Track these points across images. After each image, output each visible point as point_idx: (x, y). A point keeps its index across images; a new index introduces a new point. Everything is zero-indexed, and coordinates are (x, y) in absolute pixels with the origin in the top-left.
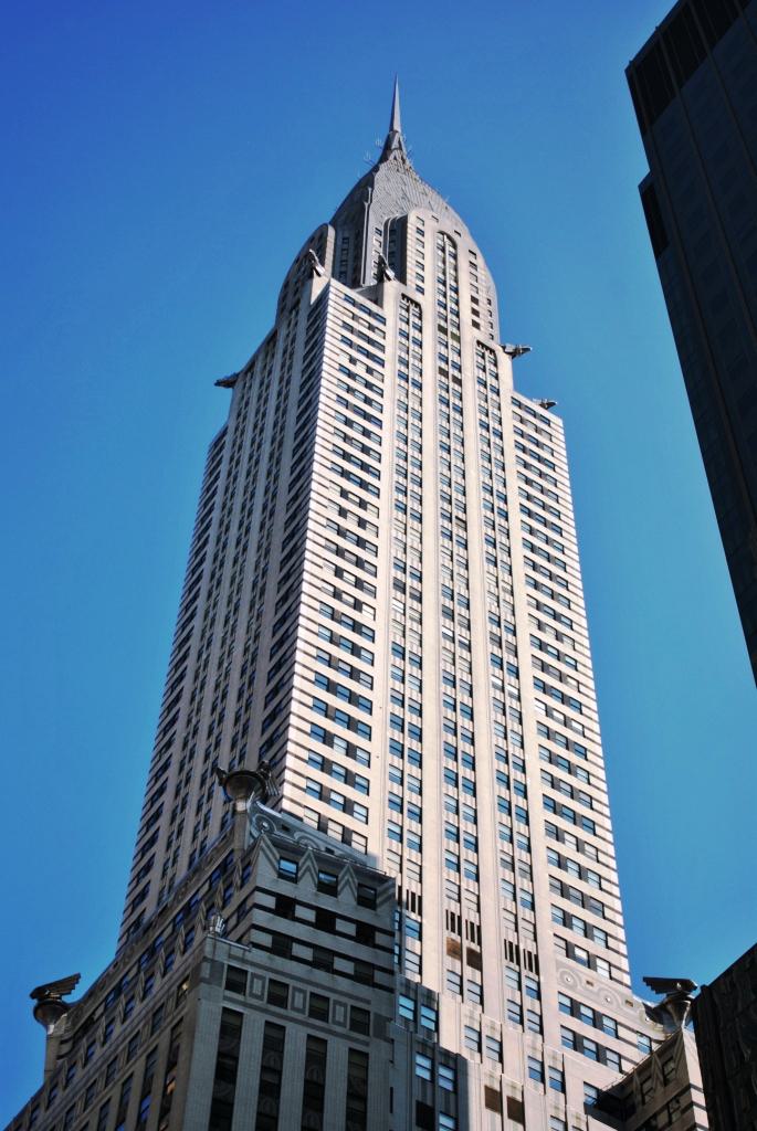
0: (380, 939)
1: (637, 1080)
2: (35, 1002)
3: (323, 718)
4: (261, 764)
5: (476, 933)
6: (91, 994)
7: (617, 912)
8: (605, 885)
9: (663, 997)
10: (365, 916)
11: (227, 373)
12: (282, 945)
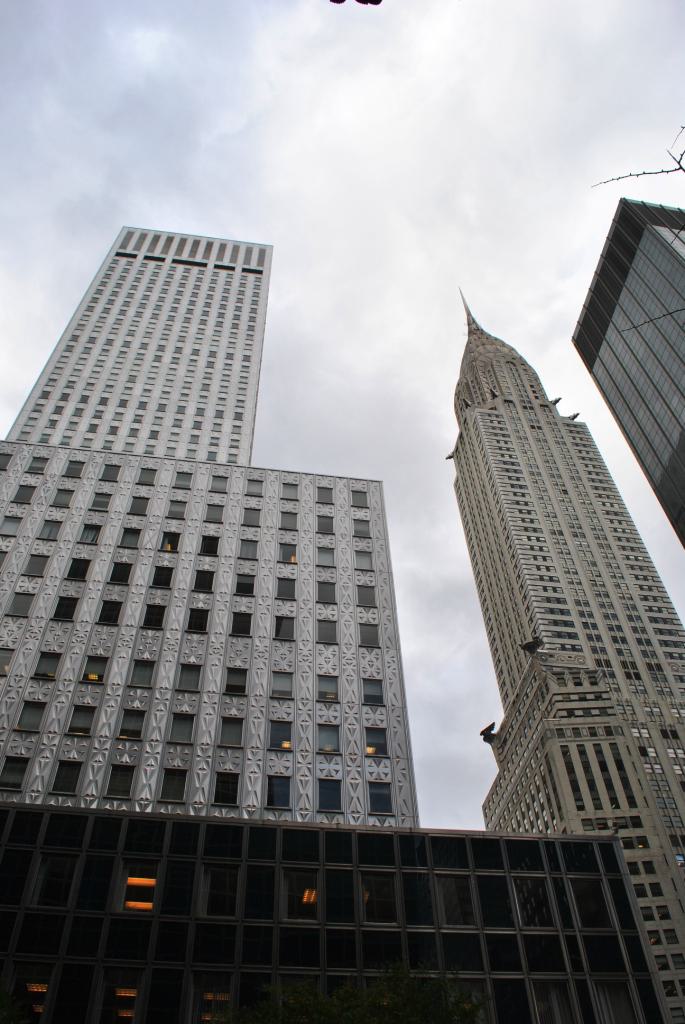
0: (604, 696)
4: (534, 638)
5: (634, 665)
6: (503, 728)
10: (595, 689)
12: (571, 713)
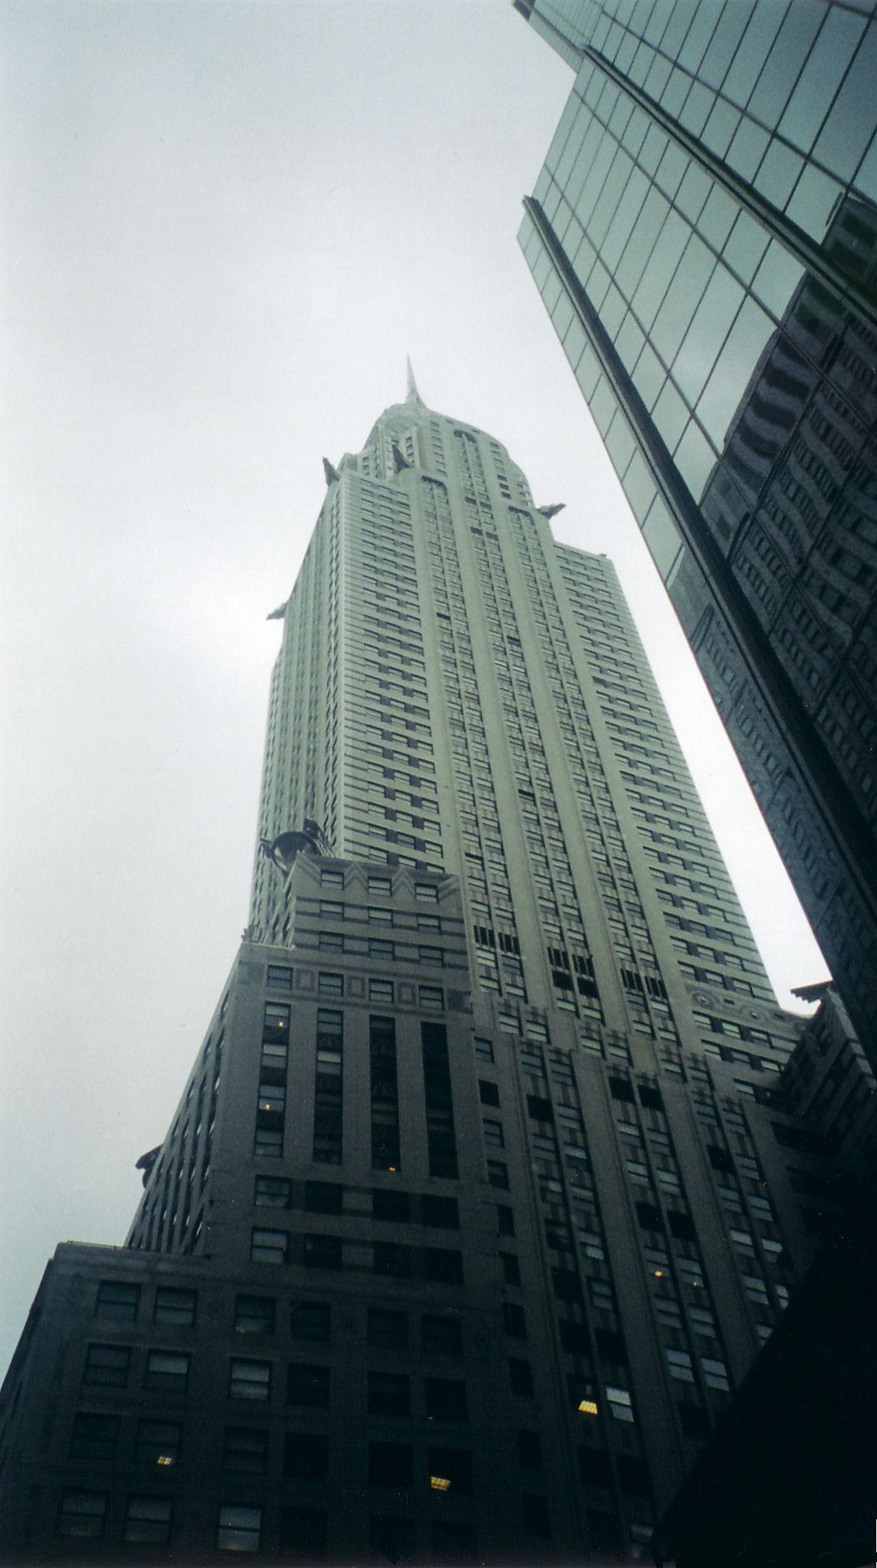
1: (795, 1066)
2: (143, 1171)
5: (586, 965)
9: (818, 1003)
11: (277, 605)
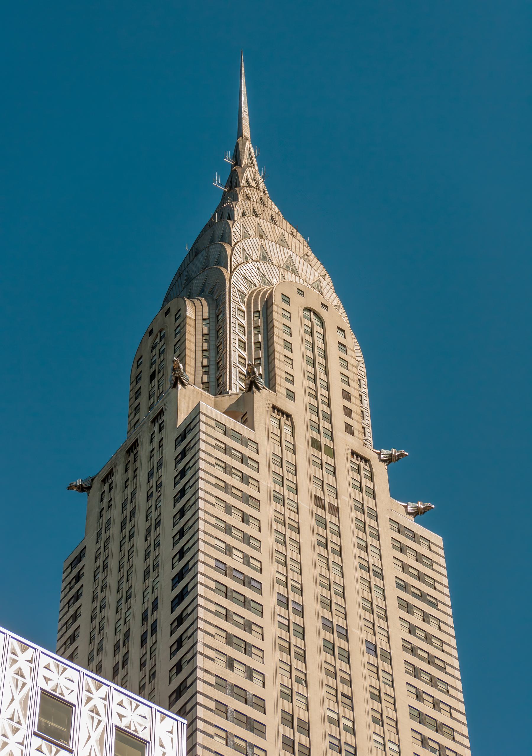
3: (224, 621)
7: (456, 669)
8: (443, 627)
